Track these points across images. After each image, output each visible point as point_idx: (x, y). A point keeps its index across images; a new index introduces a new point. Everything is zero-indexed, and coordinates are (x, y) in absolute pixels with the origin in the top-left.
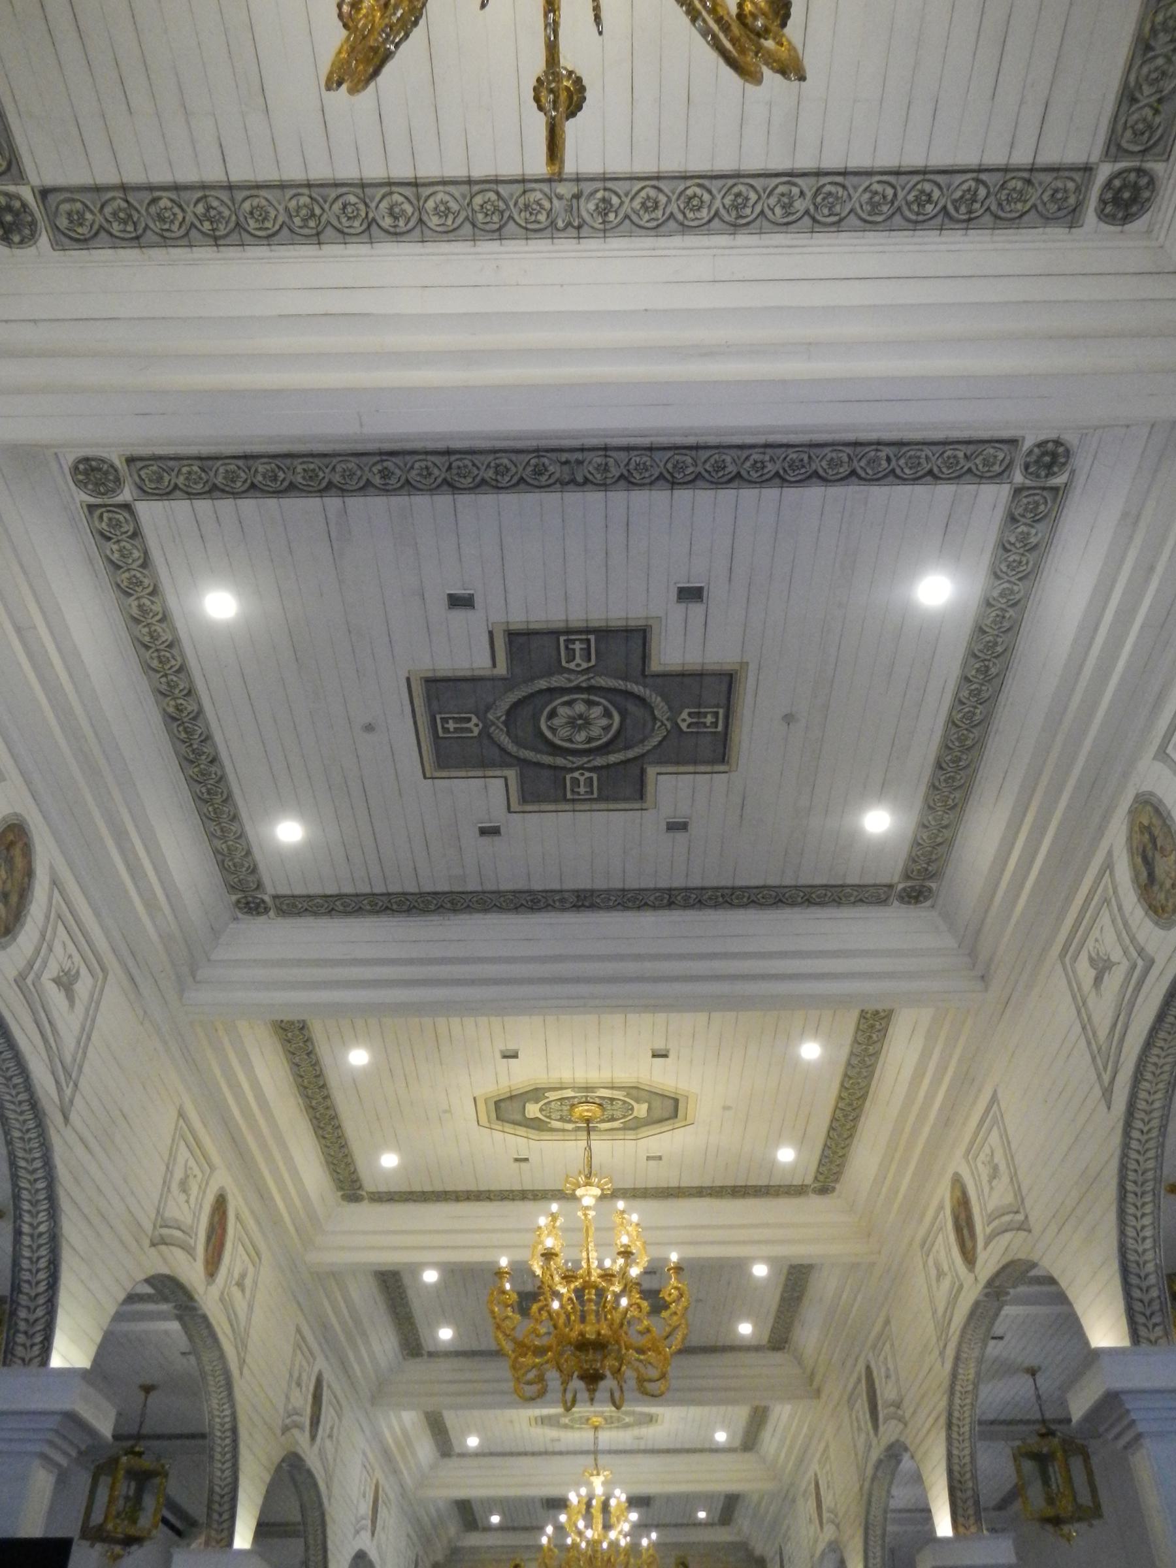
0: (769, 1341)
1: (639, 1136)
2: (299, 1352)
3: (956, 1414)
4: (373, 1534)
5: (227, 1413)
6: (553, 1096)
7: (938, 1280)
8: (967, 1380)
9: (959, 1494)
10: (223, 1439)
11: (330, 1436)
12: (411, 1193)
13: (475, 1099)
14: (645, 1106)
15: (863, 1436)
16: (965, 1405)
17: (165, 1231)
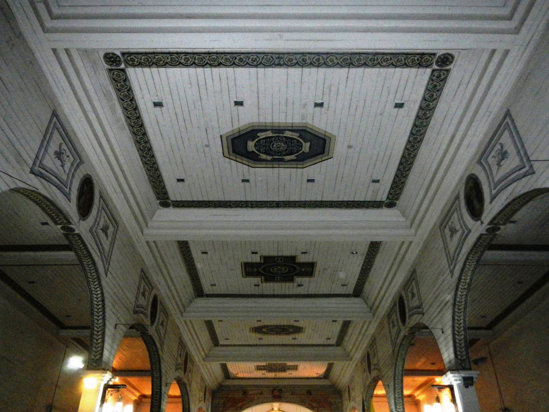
0: (353, 292)
1: (305, 165)
2: (143, 281)
3: (458, 299)
4: (185, 373)
5: (99, 292)
6: (262, 135)
7: (452, 236)
8: (466, 282)
9: (457, 337)
10: (98, 305)
11: (162, 324)
12: (193, 201)
13: (221, 136)
14: (308, 144)
15: (396, 328)
16: (463, 295)
17: (42, 170)
